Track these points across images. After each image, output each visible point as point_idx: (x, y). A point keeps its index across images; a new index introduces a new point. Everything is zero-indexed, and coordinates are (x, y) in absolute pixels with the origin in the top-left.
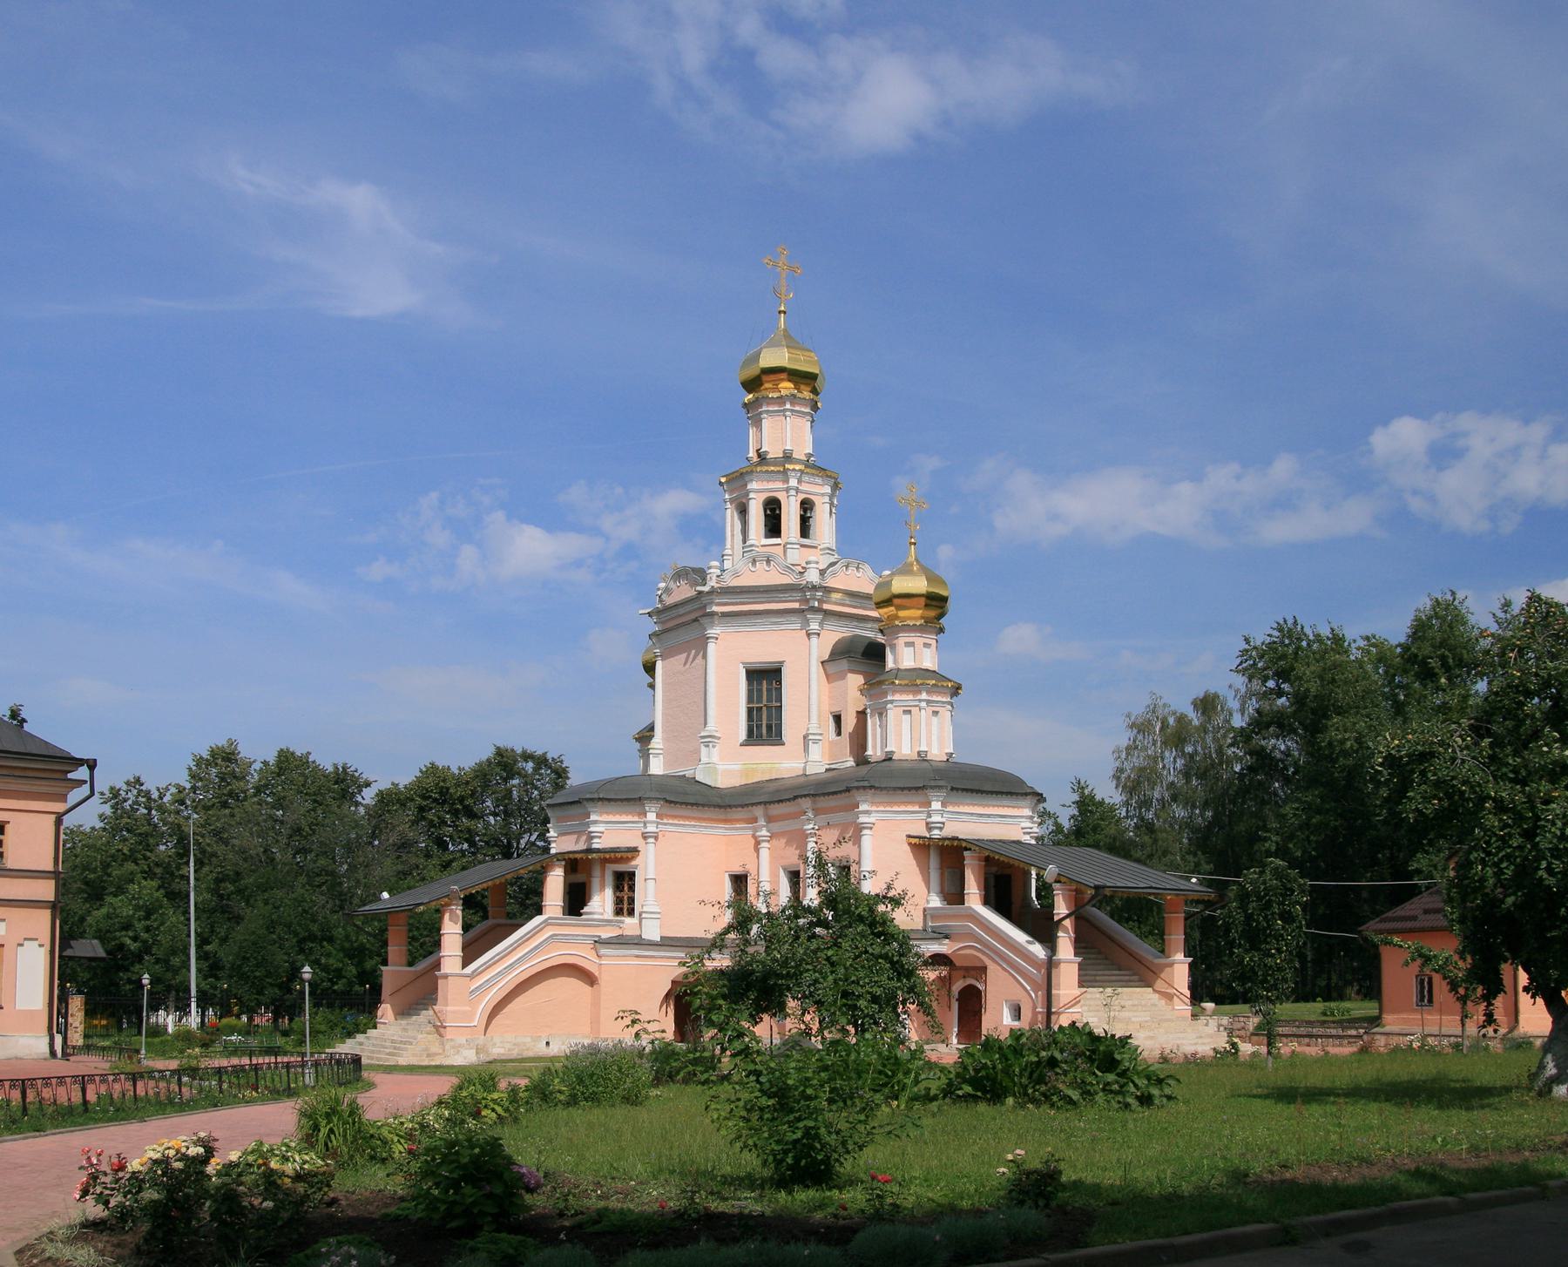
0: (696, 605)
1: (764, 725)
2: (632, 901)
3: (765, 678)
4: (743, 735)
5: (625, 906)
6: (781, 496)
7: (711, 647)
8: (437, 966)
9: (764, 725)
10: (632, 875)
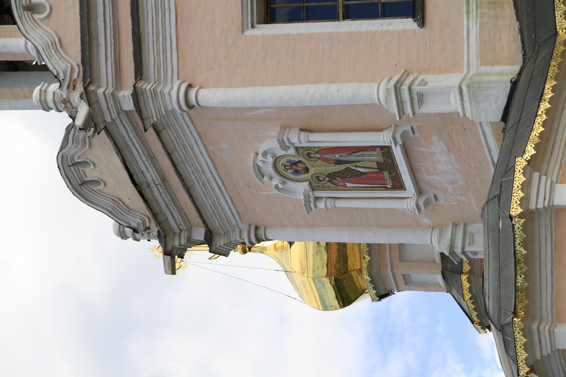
0: (126, 132)
4: (407, 24)
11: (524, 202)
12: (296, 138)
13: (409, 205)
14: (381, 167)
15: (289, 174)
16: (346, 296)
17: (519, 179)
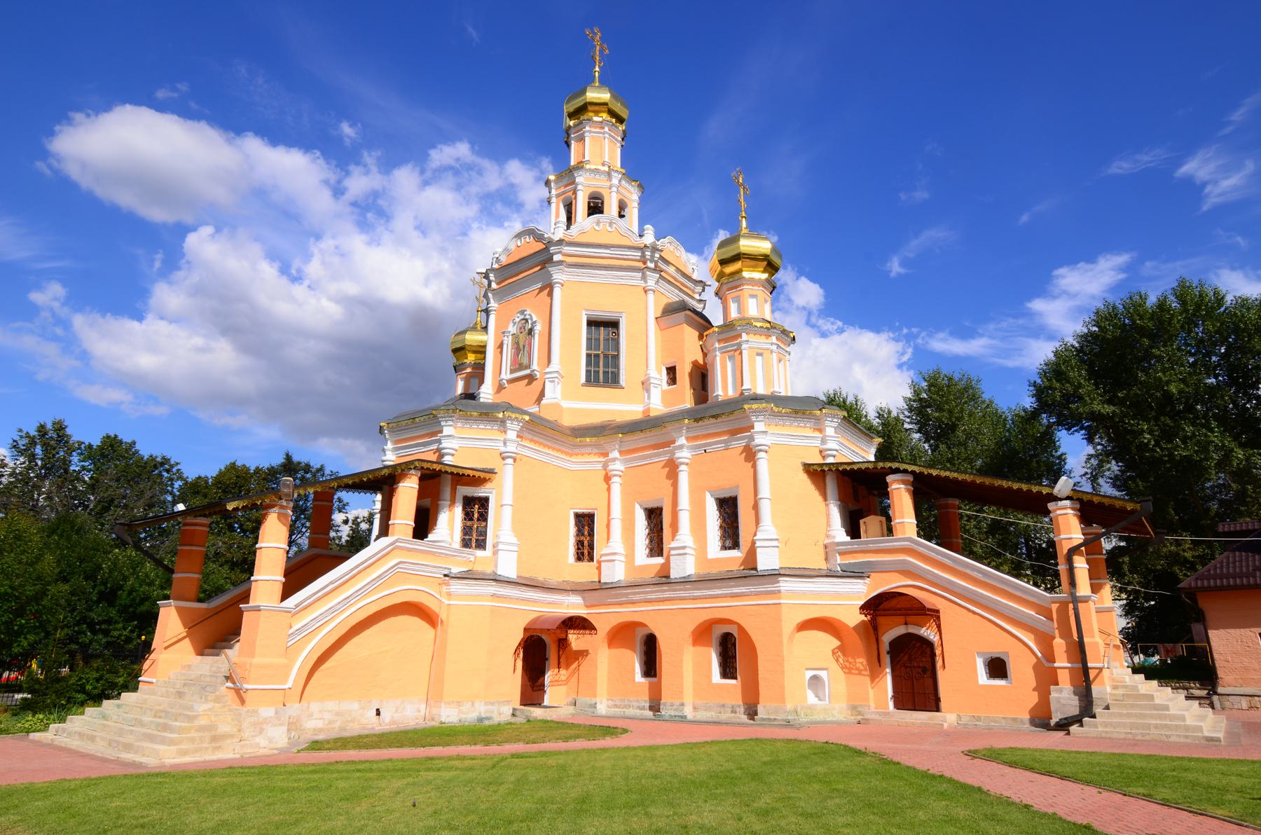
1: (603, 369)
2: (483, 533)
3: (605, 326)
4: (583, 379)
5: (474, 537)
6: (605, 193)
7: (557, 291)
8: (245, 597)
9: (603, 369)
10: (484, 502)
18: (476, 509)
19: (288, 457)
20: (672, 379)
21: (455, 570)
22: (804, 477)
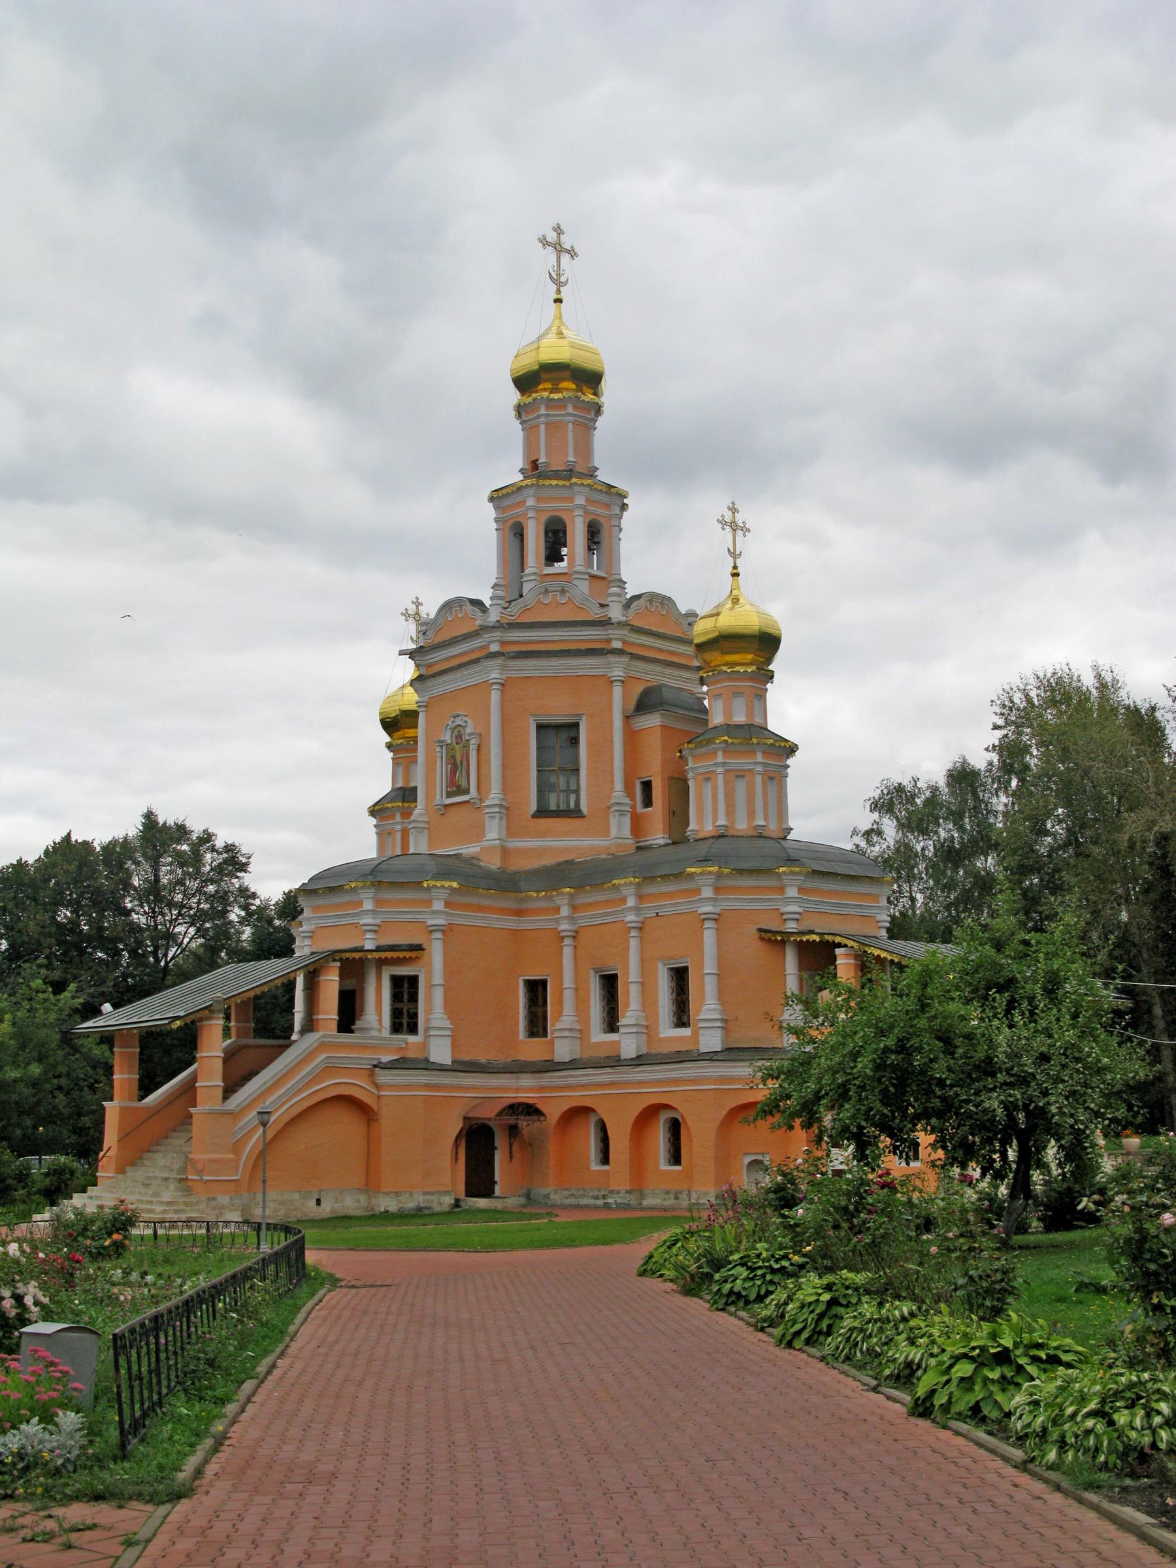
2: (414, 1016)
4: (533, 807)
5: (405, 1019)
10: (413, 981)
11: (435, 887)
12: (473, 742)
13: (438, 800)
14: (459, 787)
15: (456, 733)
16: (390, 724)
17: (447, 884)
18: (405, 990)
19: (150, 817)
20: (648, 802)
21: (386, 1059)
22: (759, 945)
